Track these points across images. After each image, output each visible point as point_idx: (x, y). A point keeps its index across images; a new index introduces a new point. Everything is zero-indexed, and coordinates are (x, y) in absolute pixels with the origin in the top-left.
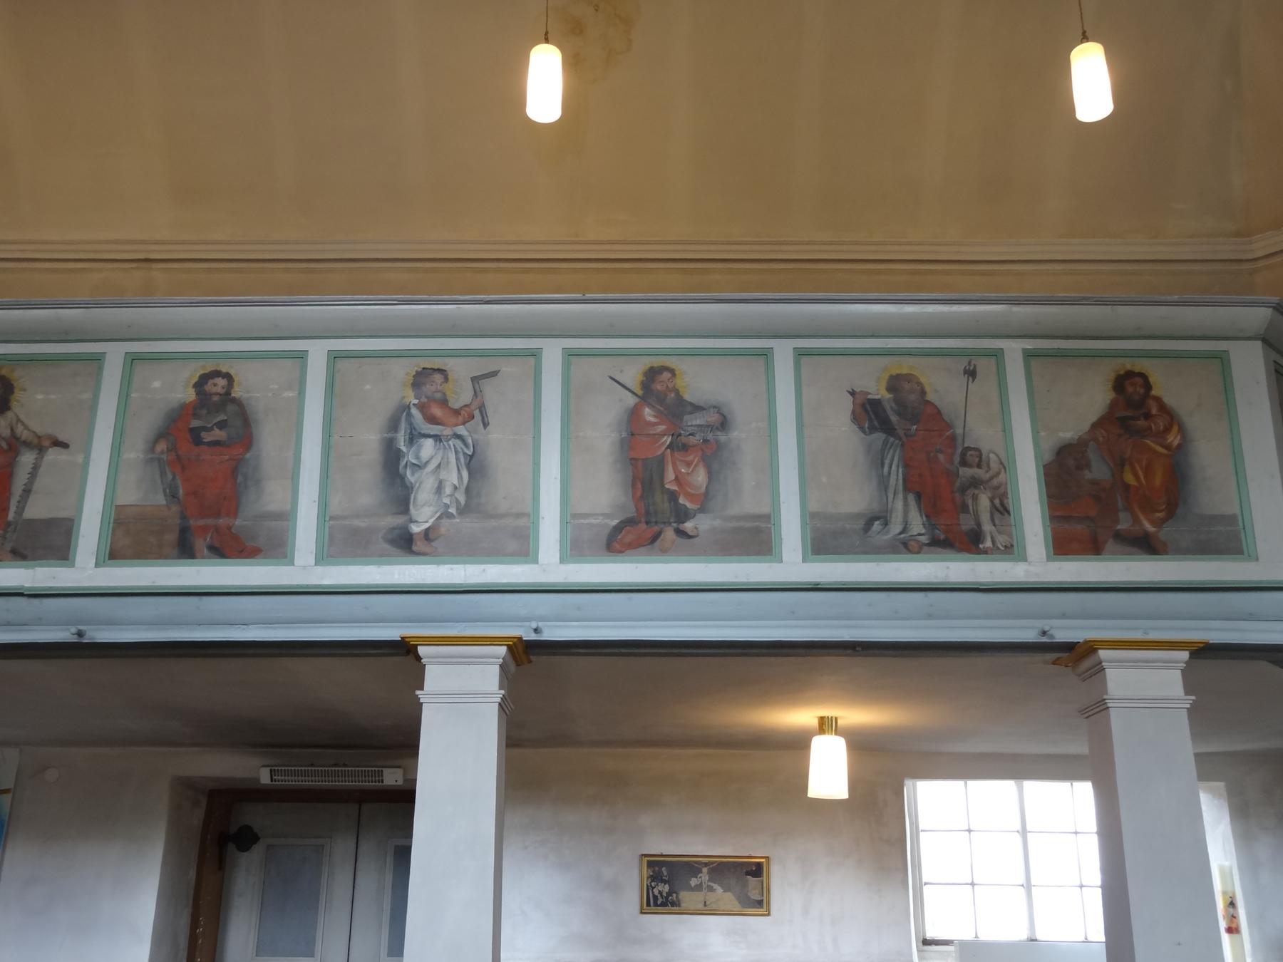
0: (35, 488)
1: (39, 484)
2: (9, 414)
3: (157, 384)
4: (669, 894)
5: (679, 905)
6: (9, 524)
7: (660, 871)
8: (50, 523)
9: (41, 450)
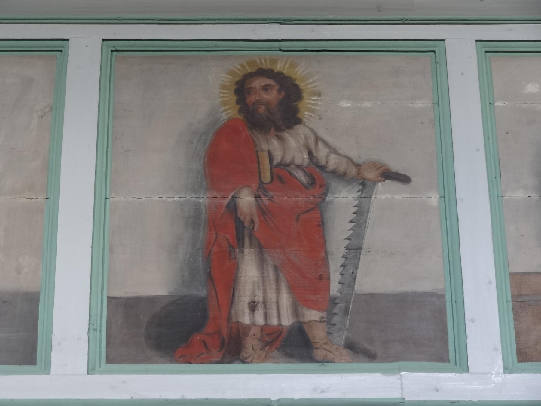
0: (366, 243)
1: (373, 237)
2: (300, 129)
3: (532, 88)
6: (334, 302)
8: (403, 301)
9: (365, 186)
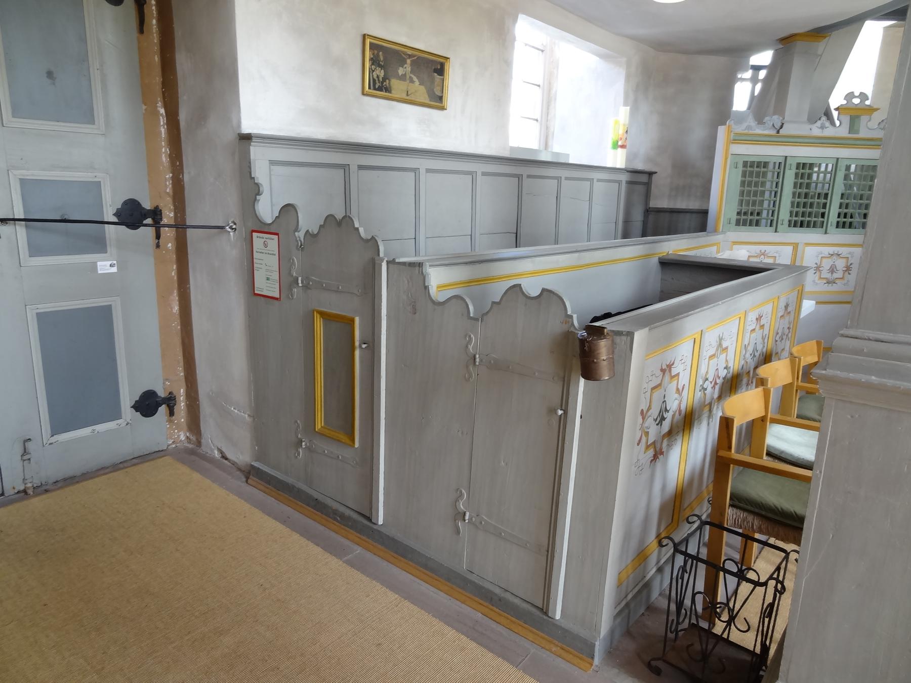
4: (384, 79)
5: (390, 92)
7: (378, 55)
